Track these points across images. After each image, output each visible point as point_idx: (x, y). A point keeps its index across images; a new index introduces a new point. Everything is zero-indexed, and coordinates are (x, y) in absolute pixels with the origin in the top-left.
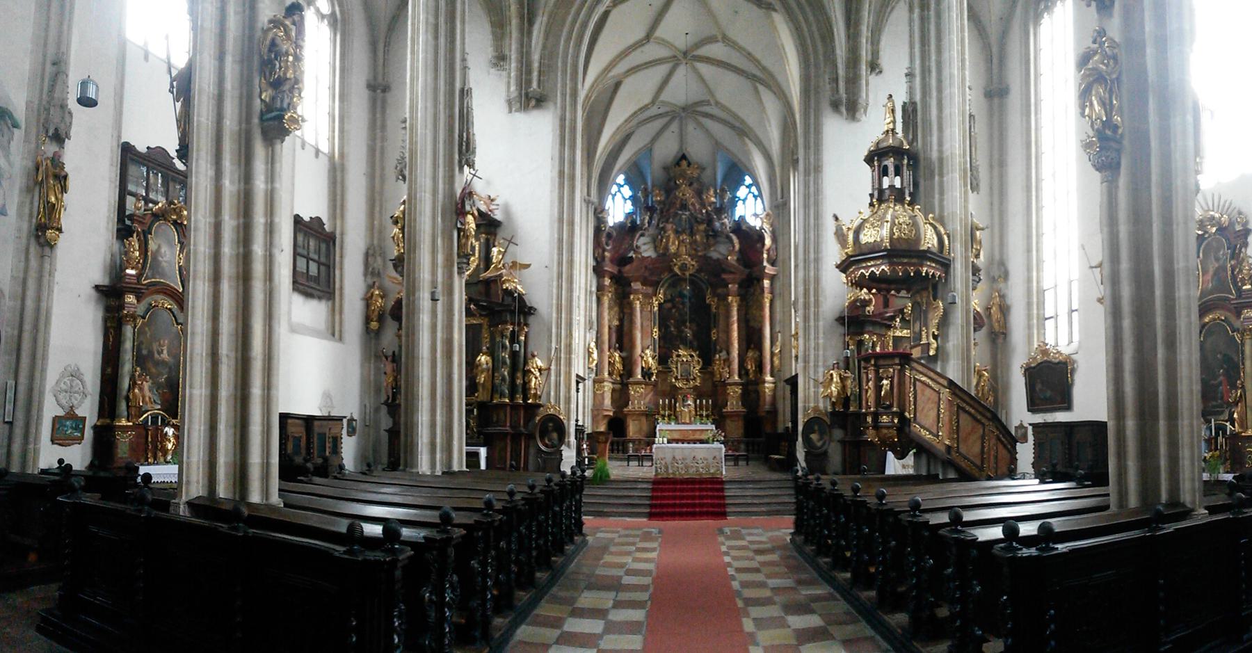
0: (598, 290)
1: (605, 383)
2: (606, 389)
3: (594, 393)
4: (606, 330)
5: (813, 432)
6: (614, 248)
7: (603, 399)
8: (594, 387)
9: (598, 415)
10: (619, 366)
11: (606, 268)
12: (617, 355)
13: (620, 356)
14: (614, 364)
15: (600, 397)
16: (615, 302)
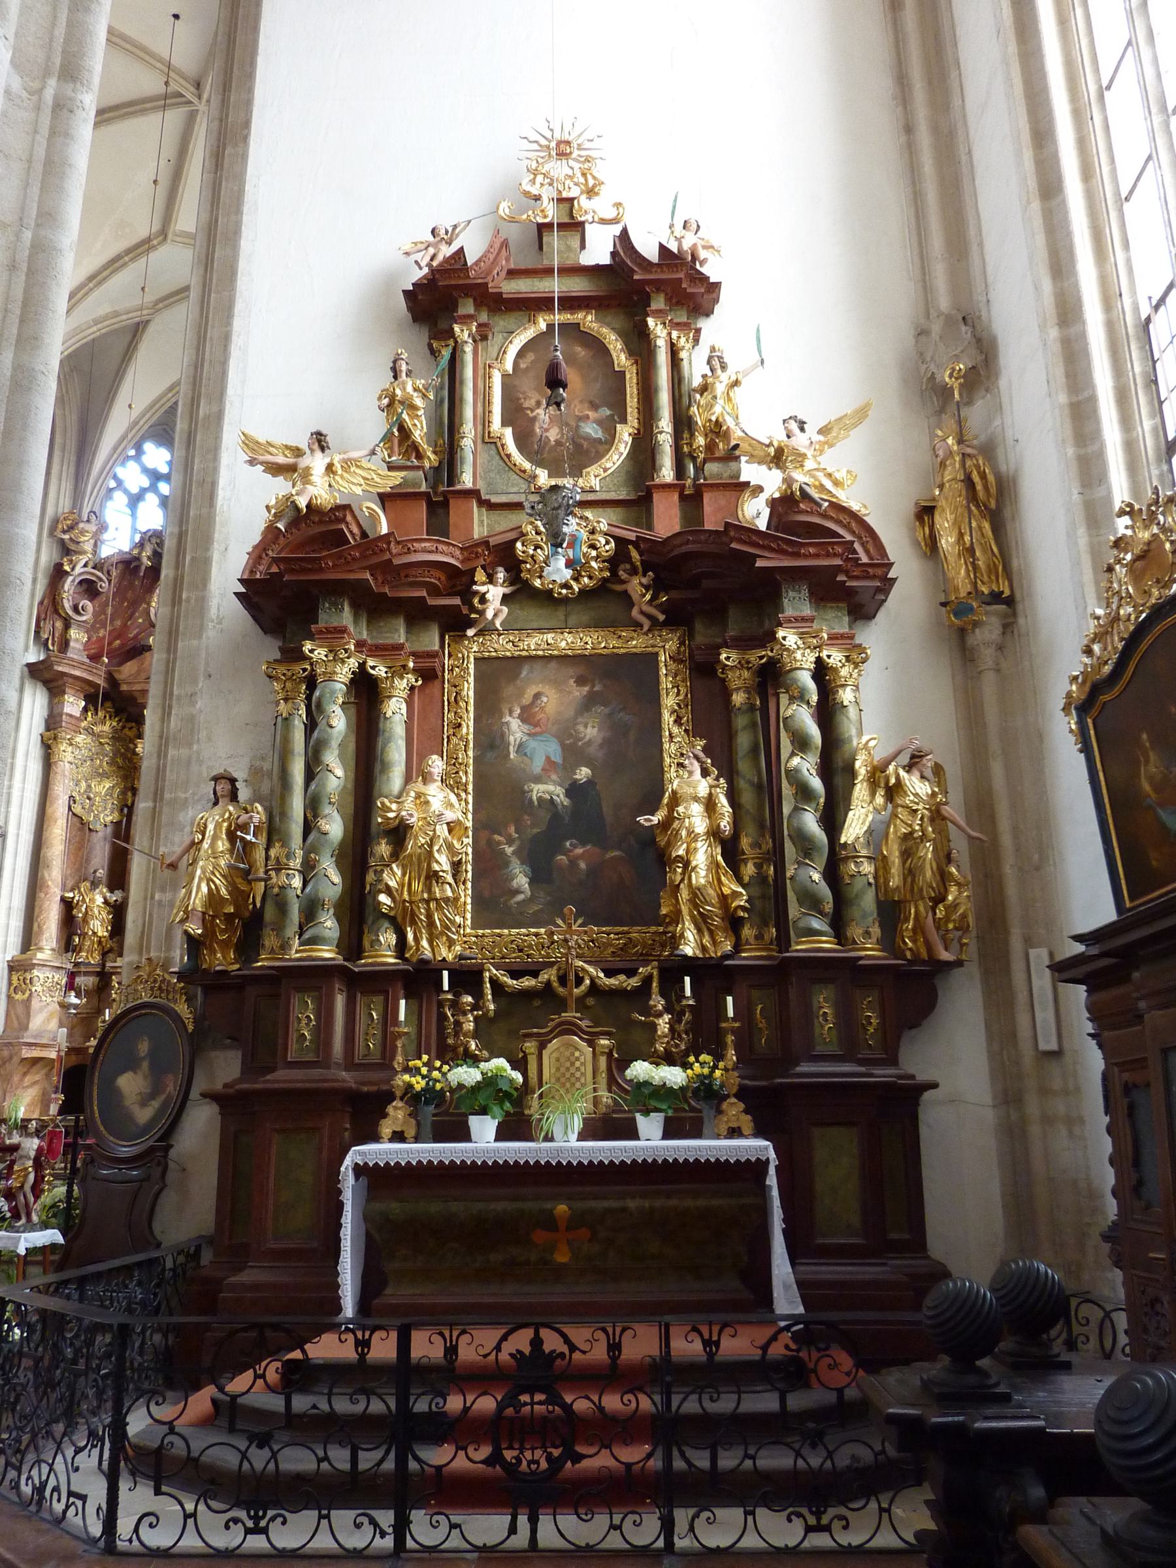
0: (48, 729)
1: (35, 972)
2: (37, 987)
3: (9, 997)
4: (58, 832)
5: (131, 1064)
6: (99, 620)
7: (28, 1015)
8: (10, 984)
9: (11, 1057)
10: (99, 926)
11: (60, 669)
12: (99, 900)
13: (106, 902)
14: (85, 920)
15: (20, 1009)
16: (111, 764)
